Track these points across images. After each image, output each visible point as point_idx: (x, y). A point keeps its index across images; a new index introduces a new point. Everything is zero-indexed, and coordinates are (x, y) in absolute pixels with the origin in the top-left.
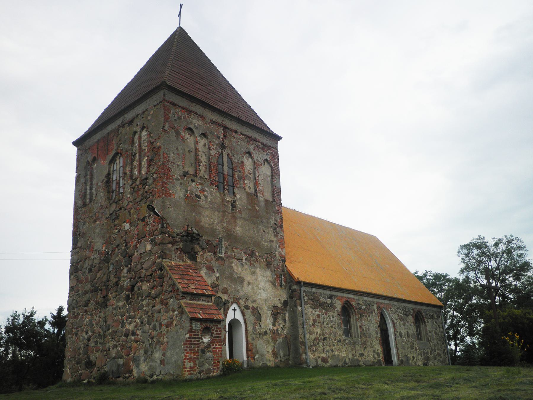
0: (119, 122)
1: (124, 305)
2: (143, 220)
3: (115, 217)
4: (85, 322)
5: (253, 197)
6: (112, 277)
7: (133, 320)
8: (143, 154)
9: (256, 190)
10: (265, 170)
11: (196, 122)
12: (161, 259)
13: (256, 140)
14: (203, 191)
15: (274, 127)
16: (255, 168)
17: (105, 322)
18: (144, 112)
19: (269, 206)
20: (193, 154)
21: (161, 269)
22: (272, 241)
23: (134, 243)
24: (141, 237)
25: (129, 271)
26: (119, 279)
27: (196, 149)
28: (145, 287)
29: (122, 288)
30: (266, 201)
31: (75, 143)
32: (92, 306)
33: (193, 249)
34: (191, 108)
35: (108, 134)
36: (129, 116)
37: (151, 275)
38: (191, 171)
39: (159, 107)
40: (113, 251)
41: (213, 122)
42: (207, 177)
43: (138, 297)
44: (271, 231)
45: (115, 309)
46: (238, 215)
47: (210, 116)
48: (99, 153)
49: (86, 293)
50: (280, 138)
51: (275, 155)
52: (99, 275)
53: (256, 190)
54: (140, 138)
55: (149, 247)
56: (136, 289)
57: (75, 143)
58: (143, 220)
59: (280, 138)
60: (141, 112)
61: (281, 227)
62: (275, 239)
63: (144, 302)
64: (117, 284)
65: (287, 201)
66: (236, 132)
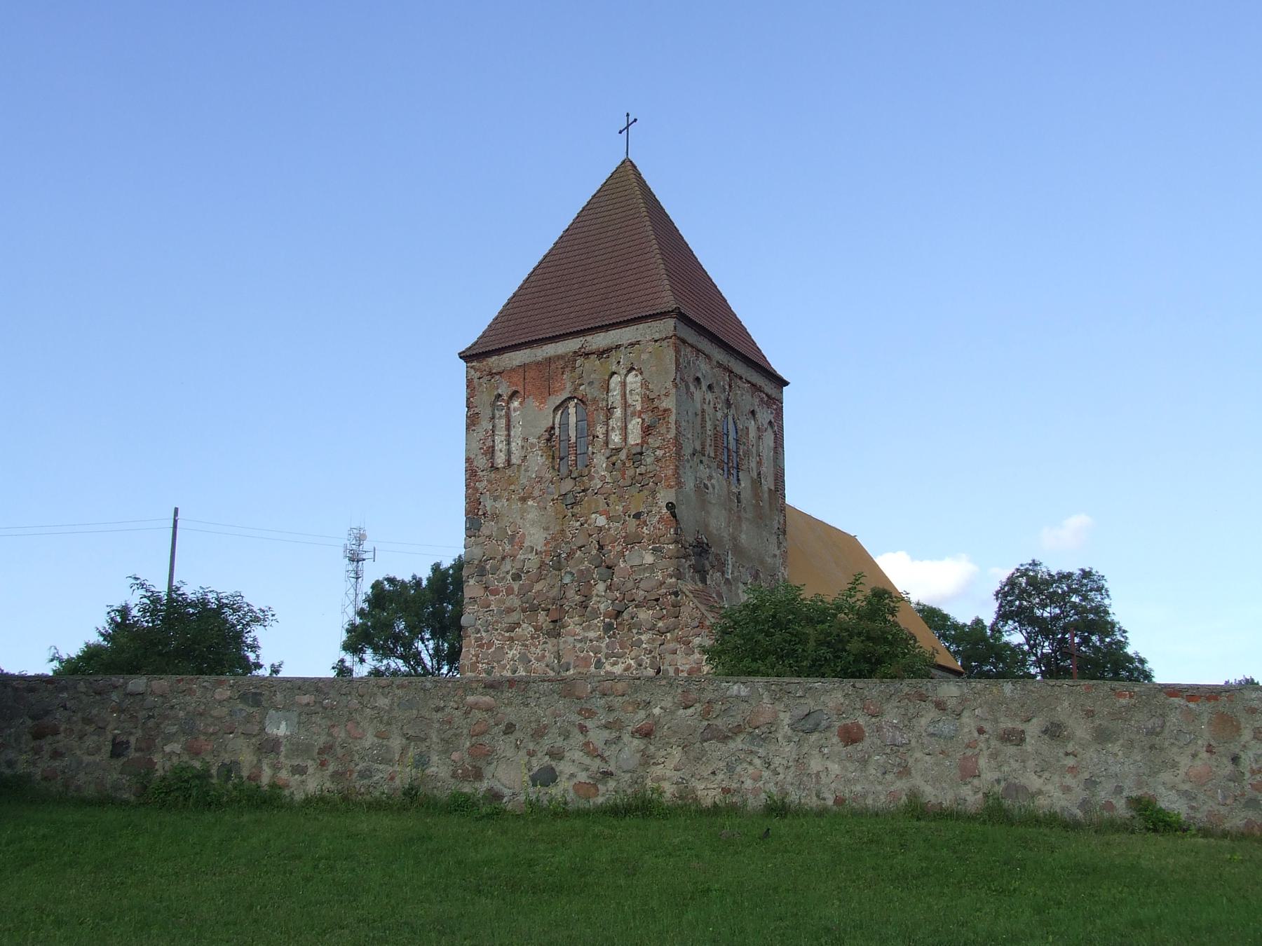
0: (572, 345)
1: (599, 639)
2: (637, 516)
3: (571, 502)
4: (510, 656)
5: (757, 483)
6: (571, 593)
7: (621, 660)
8: (629, 412)
9: (759, 474)
10: (769, 438)
11: (704, 367)
12: (674, 580)
13: (760, 389)
14: (710, 478)
15: (778, 365)
16: (759, 437)
17: (559, 657)
18: (632, 345)
19: (783, 508)
20: (699, 418)
21: (676, 594)
22: (775, 556)
23: (619, 548)
24: (632, 541)
25: (609, 588)
26: (588, 597)
27: (703, 411)
28: (644, 615)
29: (596, 614)
30: (770, 490)
31: (467, 356)
32: (526, 629)
33: (703, 566)
34: (700, 346)
35: (549, 360)
36: (600, 341)
37: (657, 600)
38: (698, 448)
39: (665, 344)
40: (570, 555)
41: (720, 365)
42: (712, 455)
43: (630, 630)
44: (774, 539)
45: (581, 641)
46: (743, 514)
47: (719, 355)
48: (528, 388)
49: (510, 610)
50: (786, 384)
51: (779, 413)
52: (538, 587)
53: (759, 474)
54: (624, 384)
55: (649, 559)
56: (625, 615)
57: (467, 356)
58: (637, 516)
59: (786, 384)
60: (625, 342)
61: (784, 533)
62: (777, 552)
63: (643, 637)
64: (584, 605)
65: (795, 496)
66: (741, 378)
